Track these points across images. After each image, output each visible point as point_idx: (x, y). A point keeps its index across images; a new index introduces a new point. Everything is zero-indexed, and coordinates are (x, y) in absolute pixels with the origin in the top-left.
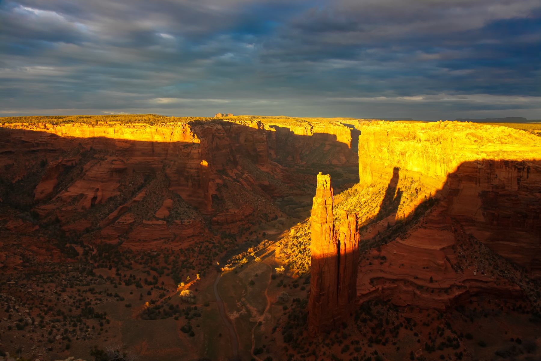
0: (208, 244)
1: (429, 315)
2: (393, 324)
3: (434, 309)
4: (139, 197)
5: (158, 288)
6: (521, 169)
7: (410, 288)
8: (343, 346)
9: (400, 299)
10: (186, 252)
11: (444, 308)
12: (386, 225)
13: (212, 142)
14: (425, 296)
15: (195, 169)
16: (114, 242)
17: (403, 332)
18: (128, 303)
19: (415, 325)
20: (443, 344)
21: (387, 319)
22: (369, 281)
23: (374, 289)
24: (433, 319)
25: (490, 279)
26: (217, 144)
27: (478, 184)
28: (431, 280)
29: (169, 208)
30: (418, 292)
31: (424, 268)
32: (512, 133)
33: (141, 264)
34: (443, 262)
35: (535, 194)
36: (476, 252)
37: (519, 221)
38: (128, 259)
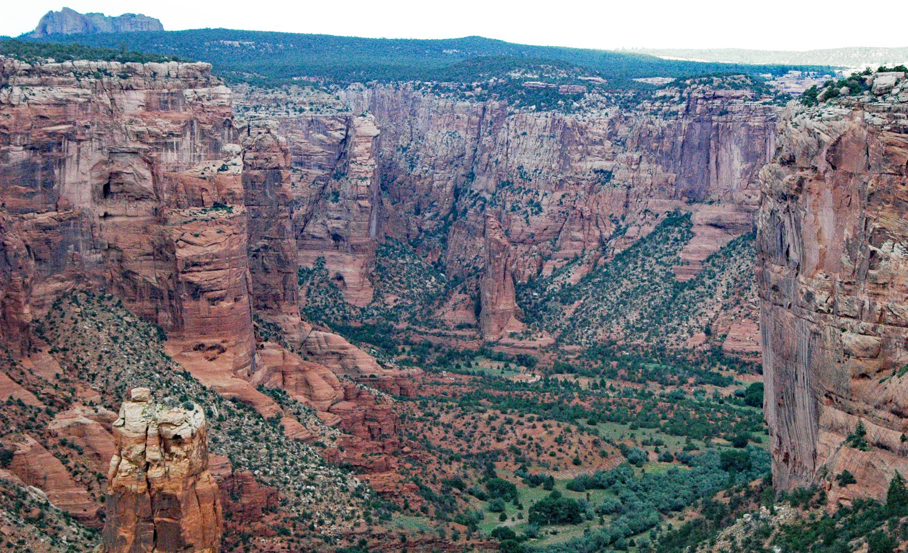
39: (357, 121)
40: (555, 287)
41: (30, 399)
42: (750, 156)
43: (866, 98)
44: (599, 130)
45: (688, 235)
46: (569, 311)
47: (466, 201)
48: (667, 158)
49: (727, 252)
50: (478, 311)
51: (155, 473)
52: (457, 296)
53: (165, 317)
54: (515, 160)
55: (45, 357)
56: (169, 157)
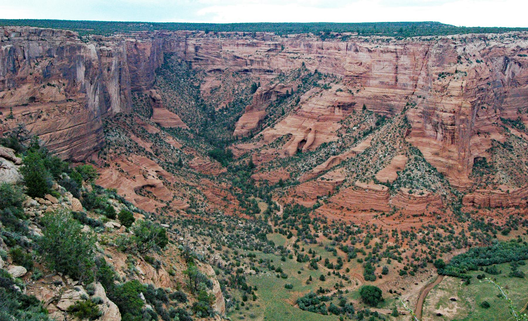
0: (441, 231)
4: (361, 147)
5: (338, 274)
10: (400, 236)
13: (503, 71)
15: (451, 112)
16: (308, 204)
18: (289, 284)
26: (513, 74)
33: (331, 239)
38: (316, 229)
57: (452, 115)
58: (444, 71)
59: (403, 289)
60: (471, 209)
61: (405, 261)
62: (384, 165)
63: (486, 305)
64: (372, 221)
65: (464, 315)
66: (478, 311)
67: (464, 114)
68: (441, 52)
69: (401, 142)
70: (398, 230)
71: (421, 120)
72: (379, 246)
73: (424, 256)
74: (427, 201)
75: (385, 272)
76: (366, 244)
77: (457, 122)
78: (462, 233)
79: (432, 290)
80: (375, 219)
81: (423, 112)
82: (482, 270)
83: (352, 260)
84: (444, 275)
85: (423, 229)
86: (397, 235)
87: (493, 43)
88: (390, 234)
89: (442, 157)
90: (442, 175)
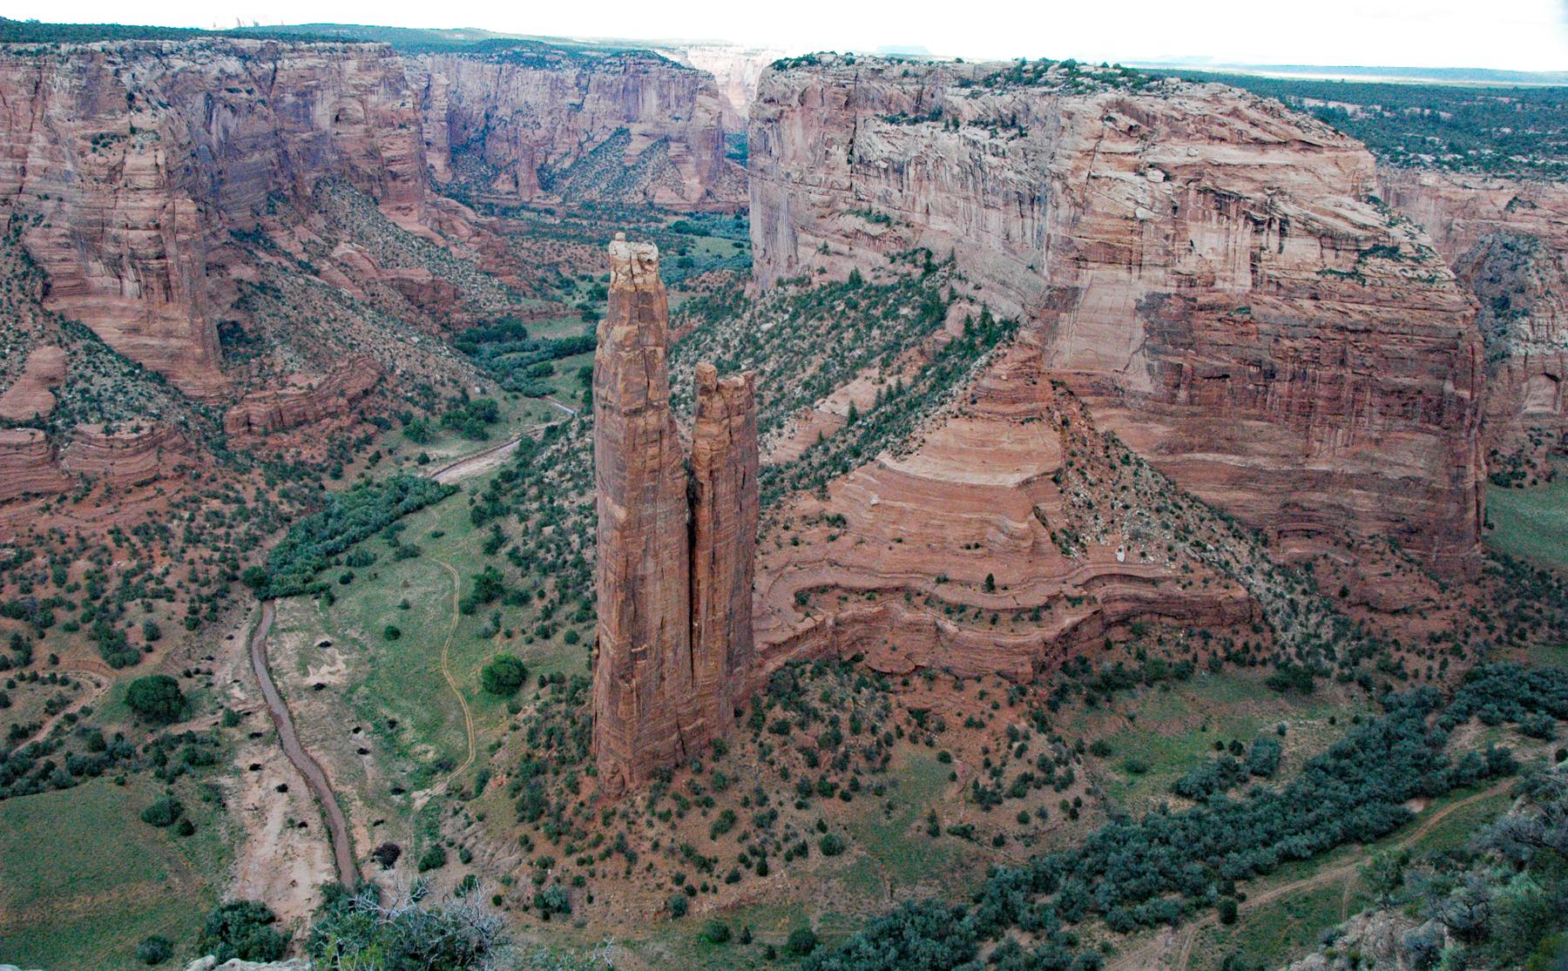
0: (216, 504)
1: (982, 695)
2: (873, 730)
3: (999, 674)
5: (35, 678)
6: (1262, 223)
7: (928, 615)
8: (715, 814)
9: (894, 649)
10: (134, 539)
11: (1028, 668)
12: (844, 410)
14: (973, 633)
15: (148, 228)
17: (903, 751)
19: (941, 729)
20: (1026, 779)
21: (853, 719)
22: (793, 600)
23: (809, 623)
24: (996, 707)
25: (1163, 572)
26: (226, 131)
27: (1135, 273)
28: (990, 585)
29: (50, 383)
30: (950, 626)
31: (968, 547)
32: (1242, 105)
34: (1024, 526)
35: (1299, 302)
36: (1124, 488)
37: (1251, 387)
39: (436, 76)
40: (556, 170)
41: (319, 240)
42: (662, 96)
43: (819, 67)
44: (571, 81)
45: (629, 141)
46: (567, 183)
47: (493, 122)
48: (615, 97)
49: (652, 149)
50: (517, 184)
51: (638, 280)
52: (504, 176)
53: (377, 191)
54: (523, 98)
55: (317, 215)
56: (373, 99)
57: (153, 233)
58: (104, 131)
59: (211, 659)
60: (249, 439)
61: (181, 594)
62: (10, 378)
63: (393, 634)
64: (43, 524)
65: (362, 668)
66: (386, 652)
67: (184, 229)
68: (84, 83)
69: (35, 315)
70: (120, 526)
71: (74, 253)
72: (96, 580)
73: (215, 570)
74: (155, 444)
75: (154, 634)
76: (60, 580)
77: (171, 249)
78: (260, 495)
79: (270, 639)
80: (46, 516)
81: (72, 235)
82: (338, 563)
83: (48, 631)
84: (273, 599)
85: (176, 511)
86: (127, 540)
87: (178, 63)
88: (109, 541)
89: (150, 335)
90: (160, 378)
